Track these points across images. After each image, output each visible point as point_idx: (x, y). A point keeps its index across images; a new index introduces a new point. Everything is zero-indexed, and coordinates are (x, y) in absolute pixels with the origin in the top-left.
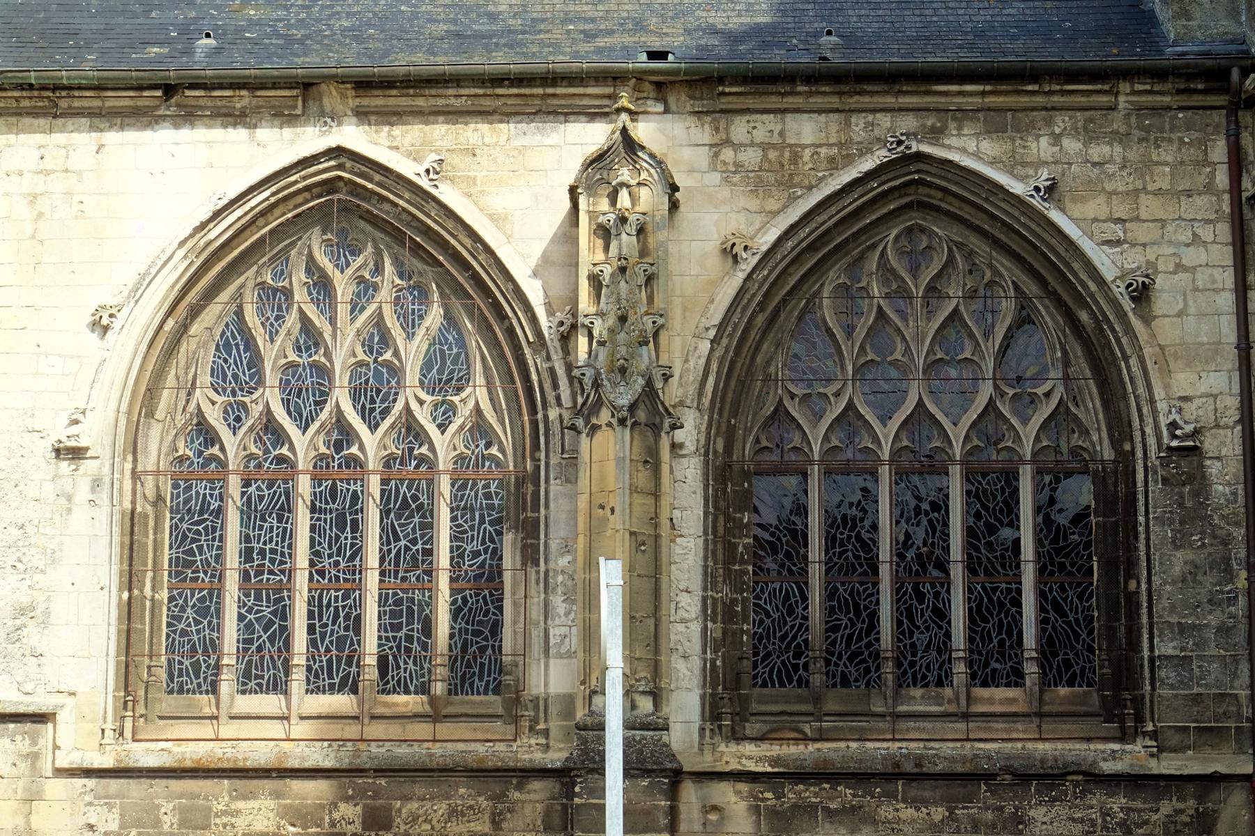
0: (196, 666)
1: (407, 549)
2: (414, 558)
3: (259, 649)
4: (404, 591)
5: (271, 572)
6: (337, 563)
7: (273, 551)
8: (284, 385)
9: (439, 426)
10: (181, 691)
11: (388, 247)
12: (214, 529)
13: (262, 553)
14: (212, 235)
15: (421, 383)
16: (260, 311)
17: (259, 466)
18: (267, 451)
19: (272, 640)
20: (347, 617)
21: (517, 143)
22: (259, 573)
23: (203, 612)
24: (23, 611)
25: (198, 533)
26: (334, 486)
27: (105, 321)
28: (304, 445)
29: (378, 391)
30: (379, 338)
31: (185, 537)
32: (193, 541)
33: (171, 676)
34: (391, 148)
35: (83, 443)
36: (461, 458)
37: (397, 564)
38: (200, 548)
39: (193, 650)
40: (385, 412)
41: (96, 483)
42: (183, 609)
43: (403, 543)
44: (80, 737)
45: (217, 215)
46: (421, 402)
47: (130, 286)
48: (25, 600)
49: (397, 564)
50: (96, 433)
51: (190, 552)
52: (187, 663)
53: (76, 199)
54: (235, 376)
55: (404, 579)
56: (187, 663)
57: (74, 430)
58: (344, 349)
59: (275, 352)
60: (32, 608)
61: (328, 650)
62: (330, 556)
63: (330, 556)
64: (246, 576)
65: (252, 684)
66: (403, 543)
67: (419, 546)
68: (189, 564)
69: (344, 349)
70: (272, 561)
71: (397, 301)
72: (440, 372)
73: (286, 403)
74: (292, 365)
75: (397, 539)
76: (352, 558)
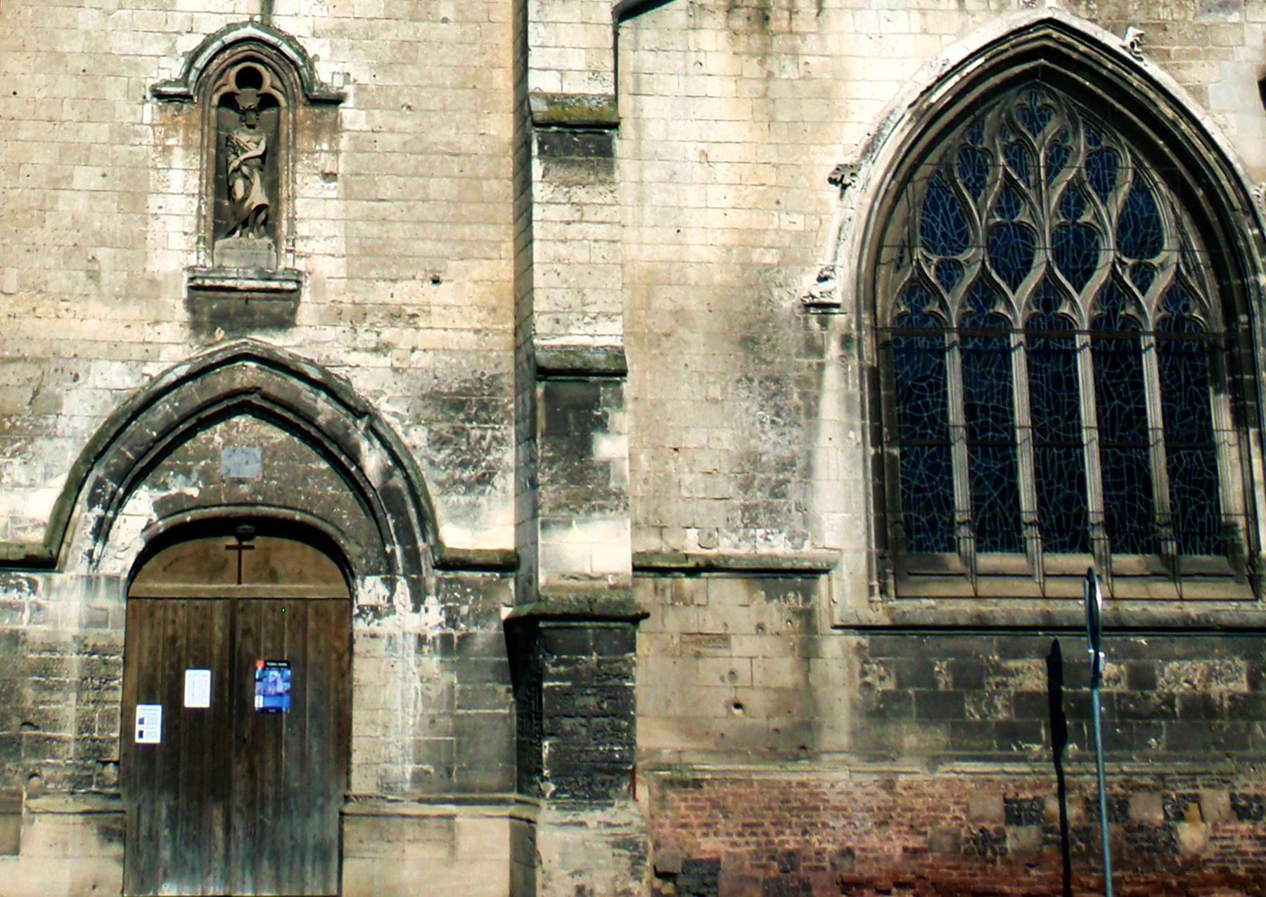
0: (932, 523)
1: (1121, 408)
2: (1128, 416)
3: (992, 507)
4: (1123, 449)
5: (995, 430)
6: (1057, 422)
7: (994, 408)
8: (990, 246)
9: (1139, 287)
10: (920, 548)
11: (1082, 111)
12: (938, 386)
13: (985, 410)
14: (934, 99)
15: (1118, 244)
16: (963, 173)
17: (974, 323)
18: (980, 309)
19: (1002, 497)
20: (1071, 476)
21: (1206, 19)
22: (984, 430)
23: (935, 468)
24: (785, 465)
25: (922, 389)
26: (1047, 343)
27: (847, 180)
28: (1018, 303)
29: (1079, 253)
30: (1074, 201)
31: (910, 393)
32: (920, 397)
33: (908, 532)
34: (1089, 20)
35: (837, 299)
36: (1164, 319)
37: (1113, 424)
38: (926, 404)
39: (928, 507)
40: (1089, 273)
41: (846, 341)
42: (915, 466)
43: (1117, 402)
44: (847, 591)
45: (941, 79)
46: (1122, 264)
47: (862, 147)
48: (786, 454)
49: (1113, 424)
50: (839, 289)
51: (916, 409)
52: (923, 519)
53: (802, 60)
54: (944, 235)
55: (1121, 438)
56: (923, 519)
57: (825, 286)
58: (1044, 213)
59: (983, 212)
60: (793, 464)
61: (1056, 508)
62: (1050, 414)
63: (1050, 414)
64: (971, 432)
65: (988, 541)
66: (1117, 402)
67: (1132, 406)
68: (915, 421)
69: (1044, 213)
70: (995, 418)
71: (1088, 165)
72: (1135, 233)
73: (994, 263)
74: (998, 225)
75: (1111, 399)
76: (1070, 417)
